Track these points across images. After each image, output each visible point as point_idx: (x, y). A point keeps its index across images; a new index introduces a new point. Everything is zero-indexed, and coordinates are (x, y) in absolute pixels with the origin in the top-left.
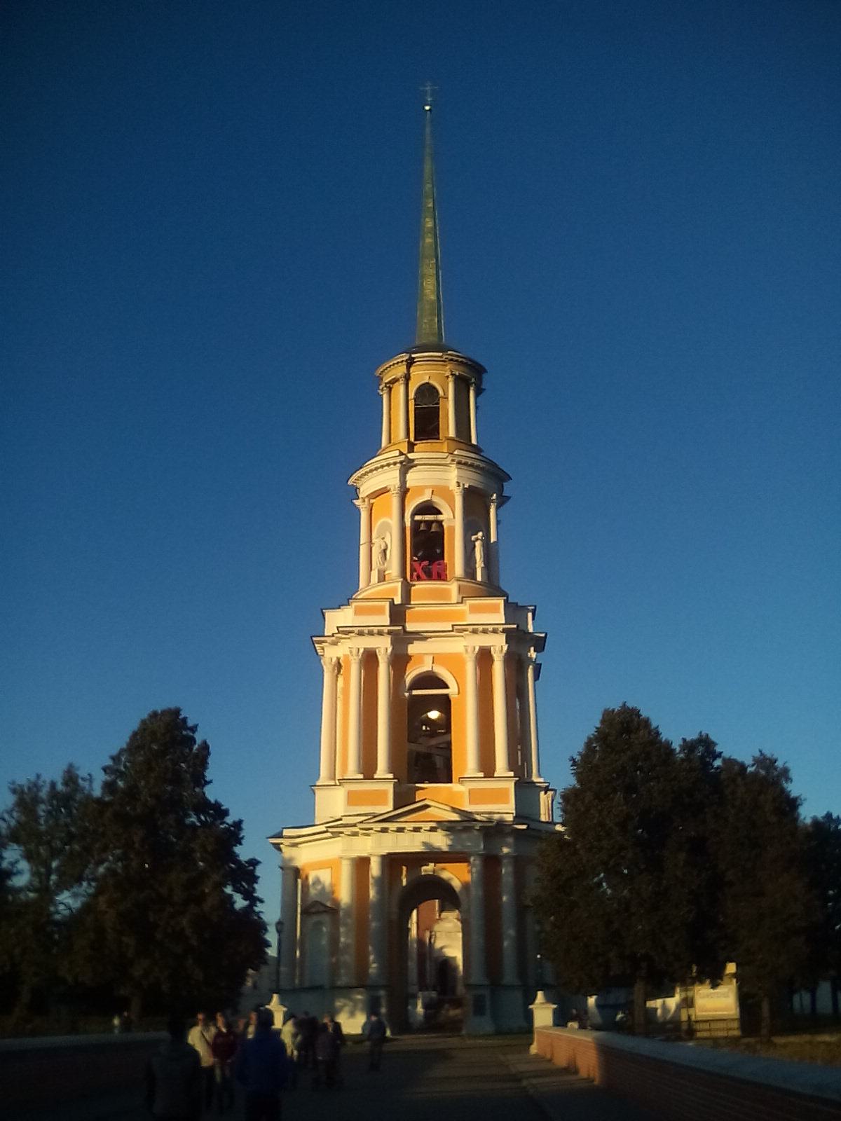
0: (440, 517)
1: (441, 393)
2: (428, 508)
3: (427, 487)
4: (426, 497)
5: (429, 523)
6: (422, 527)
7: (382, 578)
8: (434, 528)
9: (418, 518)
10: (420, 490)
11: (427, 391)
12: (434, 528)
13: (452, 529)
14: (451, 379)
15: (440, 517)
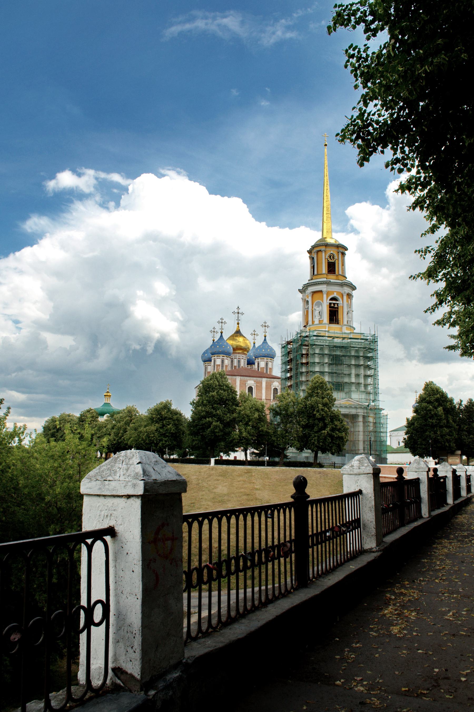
0: (337, 302)
1: (336, 257)
2: (334, 299)
3: (335, 292)
4: (335, 295)
5: (334, 304)
6: (332, 305)
7: (320, 322)
8: (336, 306)
9: (331, 302)
10: (333, 293)
11: (331, 256)
12: (336, 306)
13: (343, 307)
14: (340, 253)
15: (337, 302)
